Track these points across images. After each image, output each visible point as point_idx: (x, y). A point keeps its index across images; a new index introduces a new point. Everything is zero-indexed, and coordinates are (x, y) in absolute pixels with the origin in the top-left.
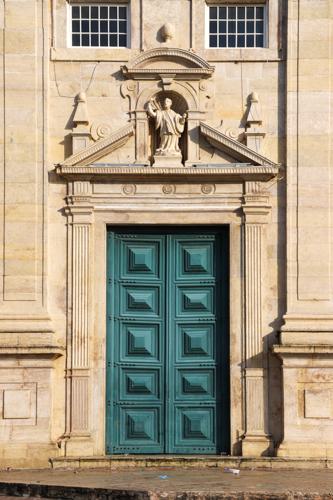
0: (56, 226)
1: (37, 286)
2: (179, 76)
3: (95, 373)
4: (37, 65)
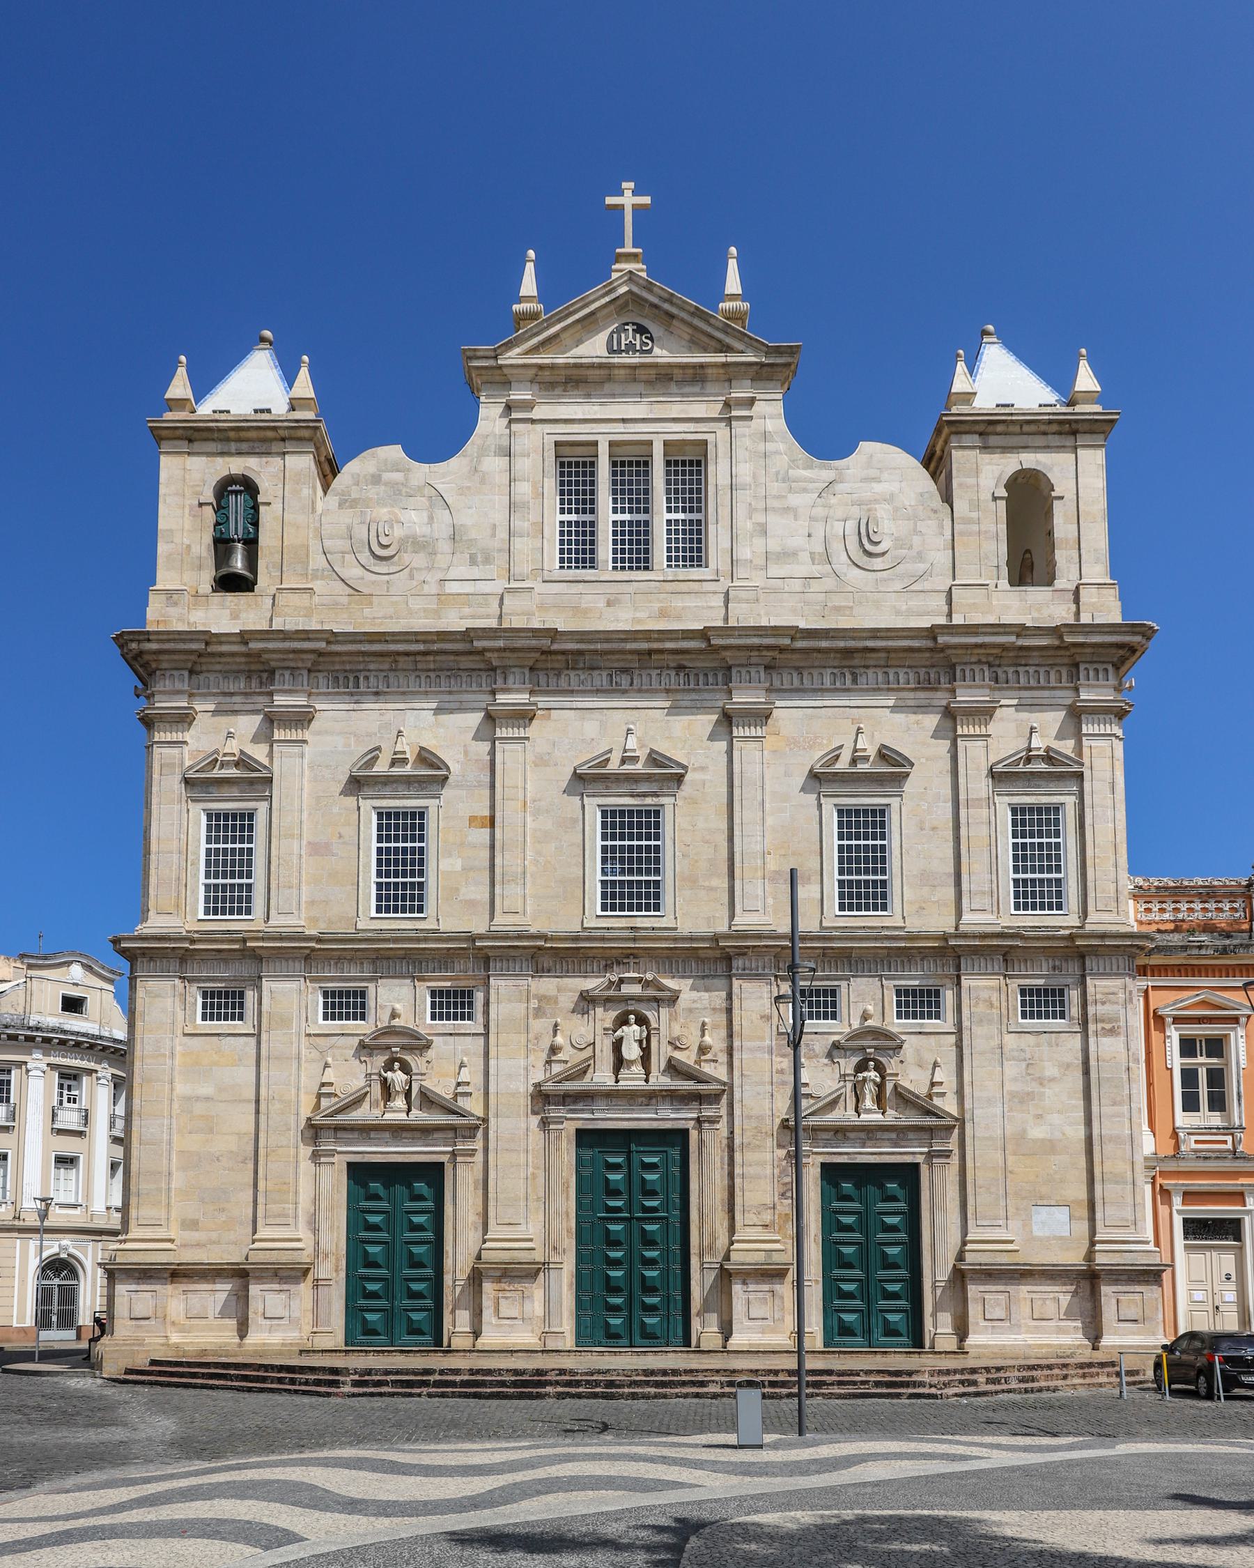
0: (306, 1166)
1: (291, 1212)
2: (403, 1048)
4: (295, 1039)
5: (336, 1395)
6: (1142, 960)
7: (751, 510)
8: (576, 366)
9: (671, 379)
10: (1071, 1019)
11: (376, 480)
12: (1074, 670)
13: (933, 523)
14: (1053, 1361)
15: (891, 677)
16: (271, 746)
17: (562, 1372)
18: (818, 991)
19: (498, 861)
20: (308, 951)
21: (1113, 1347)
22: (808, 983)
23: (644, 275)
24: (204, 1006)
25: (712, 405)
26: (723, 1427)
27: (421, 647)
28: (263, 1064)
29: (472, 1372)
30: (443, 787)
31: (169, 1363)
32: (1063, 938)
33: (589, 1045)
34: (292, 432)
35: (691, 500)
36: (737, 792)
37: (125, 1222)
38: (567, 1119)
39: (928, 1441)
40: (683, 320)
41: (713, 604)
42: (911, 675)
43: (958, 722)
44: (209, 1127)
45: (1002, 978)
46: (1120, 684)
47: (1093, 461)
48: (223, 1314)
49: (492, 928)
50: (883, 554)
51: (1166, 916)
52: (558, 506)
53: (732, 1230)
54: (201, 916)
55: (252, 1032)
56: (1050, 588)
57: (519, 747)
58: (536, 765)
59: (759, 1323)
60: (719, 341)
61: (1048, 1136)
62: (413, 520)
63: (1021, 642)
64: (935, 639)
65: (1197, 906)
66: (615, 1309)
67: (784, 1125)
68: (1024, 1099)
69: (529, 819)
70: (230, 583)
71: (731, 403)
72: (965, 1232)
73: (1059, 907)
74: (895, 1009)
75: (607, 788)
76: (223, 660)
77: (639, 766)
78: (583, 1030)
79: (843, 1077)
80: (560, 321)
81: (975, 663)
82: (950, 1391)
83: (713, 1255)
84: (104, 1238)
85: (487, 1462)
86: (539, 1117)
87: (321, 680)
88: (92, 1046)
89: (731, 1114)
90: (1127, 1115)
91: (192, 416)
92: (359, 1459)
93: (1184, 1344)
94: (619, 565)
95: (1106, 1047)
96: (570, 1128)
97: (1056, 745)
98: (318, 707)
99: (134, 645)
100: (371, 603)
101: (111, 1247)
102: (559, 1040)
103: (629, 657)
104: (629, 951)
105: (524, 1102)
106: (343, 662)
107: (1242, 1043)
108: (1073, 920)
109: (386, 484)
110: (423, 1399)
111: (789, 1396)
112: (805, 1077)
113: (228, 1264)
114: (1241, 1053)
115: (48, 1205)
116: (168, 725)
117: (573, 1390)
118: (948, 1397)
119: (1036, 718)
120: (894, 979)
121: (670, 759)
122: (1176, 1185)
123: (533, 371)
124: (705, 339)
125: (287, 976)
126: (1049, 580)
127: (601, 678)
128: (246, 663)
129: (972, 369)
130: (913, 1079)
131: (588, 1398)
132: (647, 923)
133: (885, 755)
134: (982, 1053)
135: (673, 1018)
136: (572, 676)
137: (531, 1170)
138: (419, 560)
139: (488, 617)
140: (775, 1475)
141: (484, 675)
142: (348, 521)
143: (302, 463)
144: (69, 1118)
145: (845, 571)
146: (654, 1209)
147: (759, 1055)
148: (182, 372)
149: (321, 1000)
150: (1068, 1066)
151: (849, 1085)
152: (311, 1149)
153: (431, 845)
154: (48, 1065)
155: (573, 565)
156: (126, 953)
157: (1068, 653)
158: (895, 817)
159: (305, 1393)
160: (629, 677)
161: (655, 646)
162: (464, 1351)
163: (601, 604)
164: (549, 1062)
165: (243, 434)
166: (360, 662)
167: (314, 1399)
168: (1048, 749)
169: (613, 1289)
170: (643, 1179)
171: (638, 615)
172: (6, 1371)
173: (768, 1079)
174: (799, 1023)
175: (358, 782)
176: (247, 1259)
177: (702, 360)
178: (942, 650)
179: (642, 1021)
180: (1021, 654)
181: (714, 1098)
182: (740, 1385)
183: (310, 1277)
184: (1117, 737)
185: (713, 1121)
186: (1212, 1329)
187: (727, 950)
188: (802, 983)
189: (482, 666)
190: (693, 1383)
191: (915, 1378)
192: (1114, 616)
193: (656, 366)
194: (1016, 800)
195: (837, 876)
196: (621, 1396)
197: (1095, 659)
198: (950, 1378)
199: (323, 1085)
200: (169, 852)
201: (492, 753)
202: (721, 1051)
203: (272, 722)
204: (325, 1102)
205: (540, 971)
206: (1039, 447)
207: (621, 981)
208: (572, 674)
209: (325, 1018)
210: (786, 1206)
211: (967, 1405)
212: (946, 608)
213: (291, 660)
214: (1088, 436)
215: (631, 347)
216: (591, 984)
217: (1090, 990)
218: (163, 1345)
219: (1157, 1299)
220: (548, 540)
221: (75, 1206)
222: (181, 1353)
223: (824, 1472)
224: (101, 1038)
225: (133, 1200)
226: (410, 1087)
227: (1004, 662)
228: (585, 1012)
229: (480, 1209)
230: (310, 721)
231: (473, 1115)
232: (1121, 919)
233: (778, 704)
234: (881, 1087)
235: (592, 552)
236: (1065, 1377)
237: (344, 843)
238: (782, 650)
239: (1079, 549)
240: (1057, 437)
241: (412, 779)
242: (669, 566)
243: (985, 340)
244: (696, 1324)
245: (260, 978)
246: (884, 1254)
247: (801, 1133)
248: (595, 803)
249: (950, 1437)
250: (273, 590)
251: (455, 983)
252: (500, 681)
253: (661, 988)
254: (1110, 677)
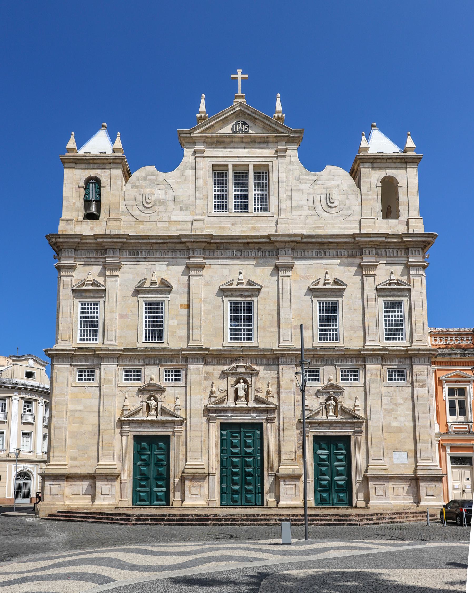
0: (118, 436)
1: (112, 454)
2: (155, 392)
3: (129, 481)
4: (114, 388)
5: (129, 524)
6: (433, 359)
7: (286, 191)
8: (220, 137)
9: (256, 142)
10: (407, 381)
11: (145, 178)
12: (407, 251)
13: (353, 196)
14: (402, 511)
15: (338, 253)
16: (105, 278)
17: (215, 515)
18: (312, 371)
19: (191, 321)
20: (119, 355)
21: (425, 506)
22: (307, 368)
23: (245, 103)
24: (79, 376)
25: (271, 152)
26: (277, 537)
27: (162, 241)
28: (102, 398)
29: (181, 515)
30: (170, 293)
31: (65, 512)
32: (404, 351)
33: (225, 391)
34: (113, 160)
35: (263, 187)
36: (281, 295)
37: (49, 458)
38: (217, 419)
39: (354, 542)
40: (260, 120)
41: (271, 225)
42: (346, 252)
43: (364, 270)
44: (81, 422)
45: (381, 366)
46: (424, 256)
47: (413, 173)
48: (86, 493)
49: (189, 347)
50: (335, 207)
51: (443, 342)
52: (214, 189)
53: (280, 461)
54: (78, 341)
55: (97, 385)
56: (398, 220)
57: (199, 278)
58: (205, 285)
59: (290, 497)
60: (274, 128)
61: (399, 426)
62: (159, 193)
63: (387, 240)
64: (355, 239)
65: (454, 339)
66: (236, 491)
67: (299, 421)
68: (390, 411)
69: (202, 306)
70: (90, 217)
71: (278, 151)
72: (368, 462)
73: (402, 339)
74: (341, 377)
75: (232, 294)
76: (87, 245)
77: (244, 286)
78: (223, 385)
79: (321, 403)
80: (214, 120)
81: (370, 248)
82: (363, 523)
83: (273, 471)
84: (41, 464)
85: (186, 550)
86: (206, 418)
87: (124, 253)
88: (37, 391)
89: (279, 417)
90: (429, 417)
91: (76, 155)
92: (137, 549)
93: (451, 505)
94: (236, 210)
95: (420, 392)
96: (218, 422)
97: (401, 278)
98: (123, 263)
99: (54, 240)
100: (143, 224)
101: (43, 468)
102: (214, 389)
103: (240, 245)
104: (240, 355)
105: (201, 412)
106: (133, 246)
107: (472, 390)
108: (407, 344)
109: (149, 180)
110: (162, 526)
111: (302, 524)
112: (307, 403)
113: (88, 474)
114: (471, 394)
115: (19, 451)
116: (66, 270)
117: (219, 522)
118: (362, 525)
119: (393, 268)
120: (340, 366)
121: (255, 283)
122: (447, 444)
123: (204, 139)
124: (269, 127)
125: (111, 364)
126: (397, 217)
127: (229, 253)
128: (96, 247)
129: (368, 139)
130: (348, 404)
131: (225, 525)
132: (247, 345)
133: (336, 282)
134: (374, 394)
135: (257, 380)
136: (219, 252)
137: (203, 438)
138: (161, 208)
139: (187, 230)
140: (295, 555)
141: (186, 251)
142: (135, 194)
143: (118, 172)
144: (28, 418)
145: (321, 213)
146: (250, 453)
147: (289, 395)
148: (72, 138)
149: (124, 373)
150: (406, 399)
151: (324, 406)
152: (120, 430)
153: (165, 315)
154: (20, 398)
155: (219, 210)
156: (49, 355)
157: (404, 244)
158: (340, 305)
159: (117, 524)
160: (240, 253)
161: (250, 241)
162: (178, 507)
163: (230, 225)
164: (210, 397)
165: (95, 161)
166: (139, 246)
167: (120, 526)
168: (397, 280)
169: (235, 484)
170: (246, 442)
171: (243, 229)
172: (2, 515)
173: (293, 404)
174: (304, 383)
175: (138, 291)
176: (95, 472)
177: (267, 135)
178: (357, 243)
179: (245, 382)
180: (387, 244)
181: (273, 411)
182: (283, 520)
183: (119, 479)
184: (423, 275)
185: (272, 419)
186: (462, 499)
187: (277, 355)
188: (305, 368)
189: (185, 248)
190: (265, 520)
191: (349, 518)
192: (422, 231)
193: (250, 137)
194: (386, 299)
195: (318, 327)
196: (238, 525)
197: (414, 246)
198: (363, 518)
199: (124, 406)
200: (66, 317)
201: (189, 280)
202: (275, 393)
203: (105, 268)
204: (125, 412)
205: (206, 363)
206: (393, 168)
207: (237, 366)
208: (219, 251)
209: (125, 380)
210: (300, 452)
211: (369, 528)
212: (359, 227)
213: (113, 245)
214: (411, 164)
215: (241, 130)
216: (226, 368)
217: (414, 370)
218: (63, 505)
219: (441, 487)
220: (210, 201)
221: (30, 452)
222: (70, 508)
223: (314, 554)
224: (40, 387)
225: (52, 450)
226: (158, 406)
227: (381, 247)
228: (224, 378)
229: (184, 453)
230: (120, 268)
231: (181, 417)
232: (426, 343)
233: (296, 263)
234: (336, 407)
235: (226, 205)
236: (406, 517)
237: (133, 314)
238: (297, 242)
239: (408, 206)
240: (399, 164)
241: (158, 290)
242: (255, 211)
243: (372, 128)
244: (266, 497)
245: (101, 365)
246: (337, 470)
247: (305, 424)
248: (228, 299)
249: (363, 541)
250: (106, 219)
251: (175, 367)
252: (191, 254)
253: (252, 369)
254: (420, 253)
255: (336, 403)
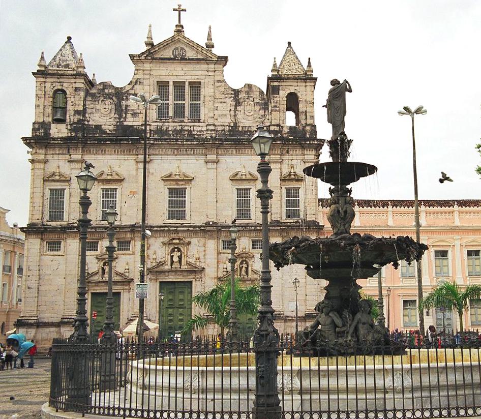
179: (179, 250)
234: (247, 268)
255: (248, 265)
